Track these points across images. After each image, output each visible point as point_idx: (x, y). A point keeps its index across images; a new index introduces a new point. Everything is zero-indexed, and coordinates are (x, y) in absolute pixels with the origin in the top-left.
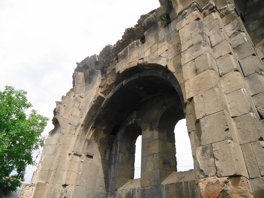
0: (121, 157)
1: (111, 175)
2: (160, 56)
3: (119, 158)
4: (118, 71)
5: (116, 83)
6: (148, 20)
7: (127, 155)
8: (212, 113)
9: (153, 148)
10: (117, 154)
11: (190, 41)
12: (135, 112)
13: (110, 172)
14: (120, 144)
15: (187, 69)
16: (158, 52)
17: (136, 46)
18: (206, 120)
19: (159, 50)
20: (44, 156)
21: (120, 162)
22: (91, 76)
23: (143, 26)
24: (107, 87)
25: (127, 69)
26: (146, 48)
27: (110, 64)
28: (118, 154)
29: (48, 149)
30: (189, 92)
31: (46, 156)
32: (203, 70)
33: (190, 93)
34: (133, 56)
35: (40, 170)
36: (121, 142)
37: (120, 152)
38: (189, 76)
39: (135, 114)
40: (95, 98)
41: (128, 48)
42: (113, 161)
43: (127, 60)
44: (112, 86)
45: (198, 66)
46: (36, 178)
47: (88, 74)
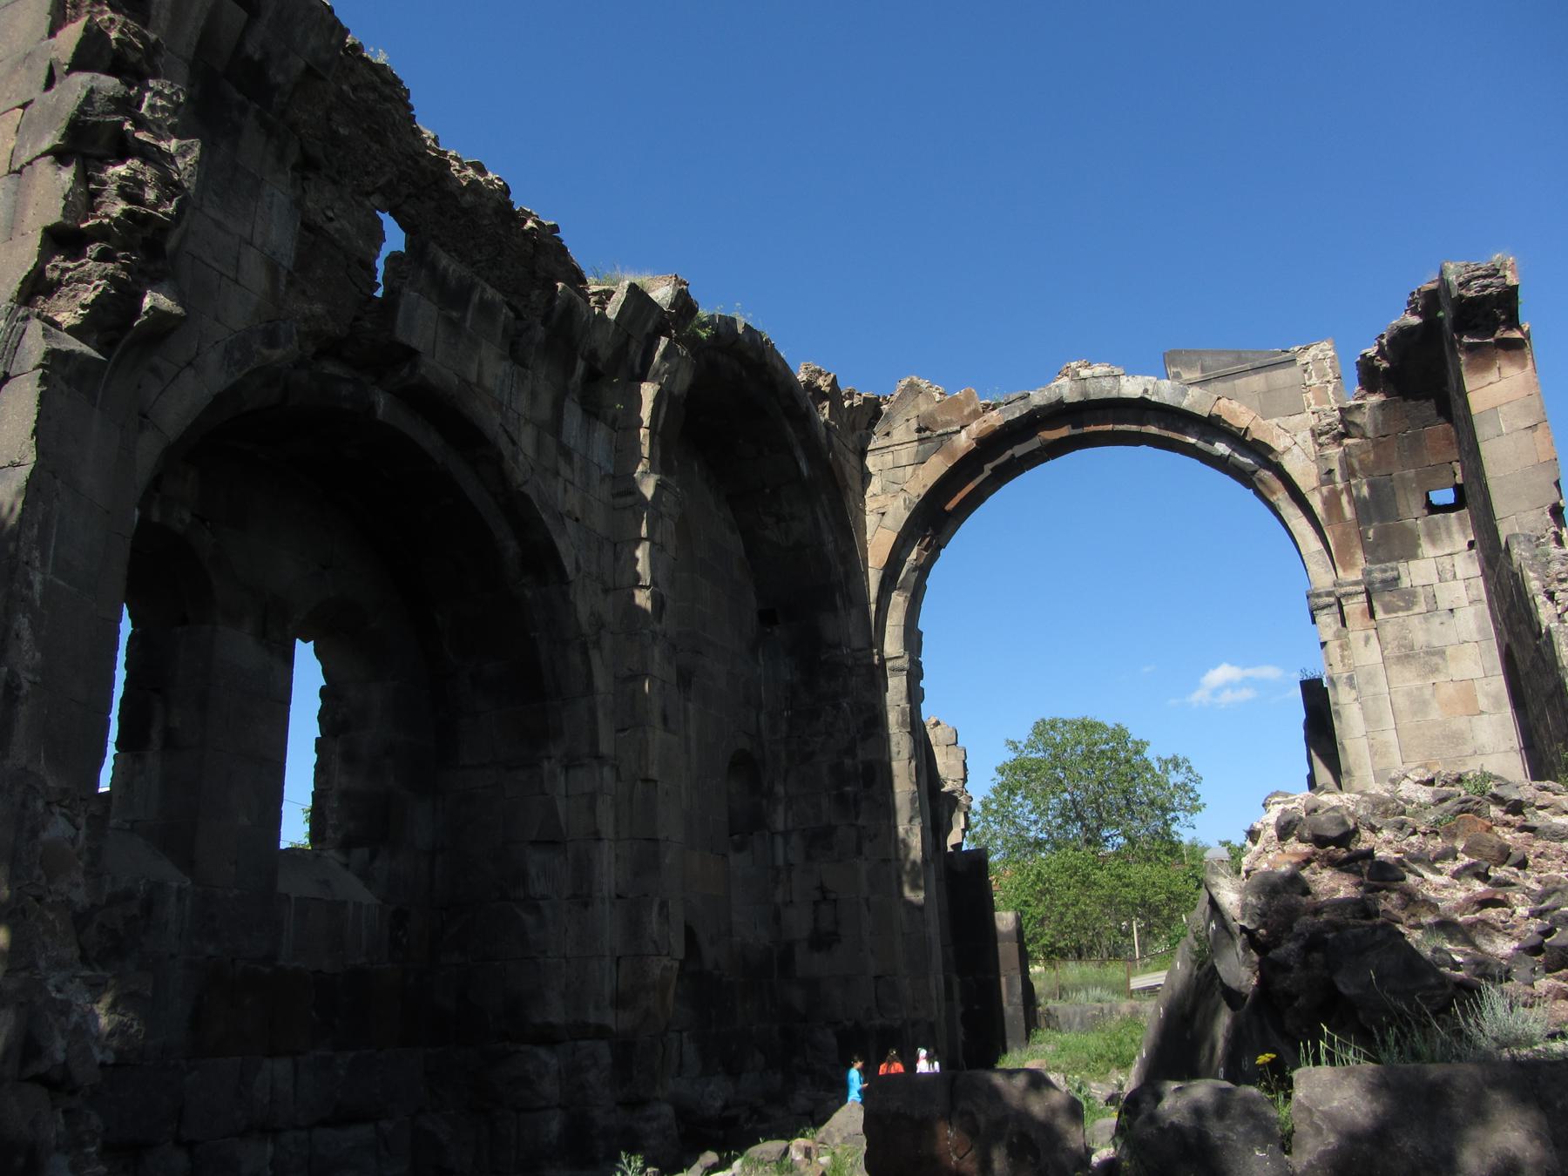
4: (416, 343)
34: (480, 365)
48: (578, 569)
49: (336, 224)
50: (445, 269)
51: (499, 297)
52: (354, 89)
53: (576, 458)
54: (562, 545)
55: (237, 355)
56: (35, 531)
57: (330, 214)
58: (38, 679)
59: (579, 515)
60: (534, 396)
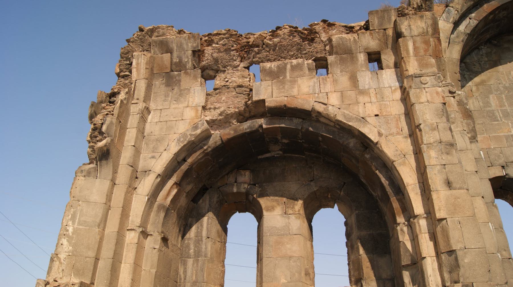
0: (209, 248)
1: (187, 276)
2: (363, 118)
3: (206, 248)
4: (262, 98)
5: (242, 116)
6: (341, 38)
7: (218, 245)
8: (473, 247)
9: (288, 246)
10: (202, 241)
11: (436, 133)
12: (247, 173)
13: (185, 272)
14: (208, 222)
15: (435, 174)
16: (358, 108)
17: (307, 72)
18: (465, 253)
19: (361, 105)
20: (73, 223)
21: (209, 256)
22: (176, 73)
23: (322, 39)
24: (220, 115)
25: (285, 106)
26: (329, 87)
27: (228, 70)
28: (204, 239)
29: (82, 210)
30: (440, 210)
31: (79, 224)
32: (458, 186)
33: (442, 211)
34: (299, 87)
35: (66, 252)
36: (210, 220)
37: (208, 238)
38: (439, 188)
39: (245, 177)
40: (196, 127)
41: (289, 66)
42: (192, 251)
43: (284, 87)
44: (232, 117)
45: (451, 179)
46: (61, 269)
47: (167, 63)
48: (380, 134)
49: (230, 81)
50: (270, 68)
51: (300, 60)
52: (217, 44)
53: (372, 91)
54: (365, 130)
55: (182, 139)
56: (70, 216)
57: (227, 80)
58: (70, 254)
59: (376, 113)
60: (335, 81)
